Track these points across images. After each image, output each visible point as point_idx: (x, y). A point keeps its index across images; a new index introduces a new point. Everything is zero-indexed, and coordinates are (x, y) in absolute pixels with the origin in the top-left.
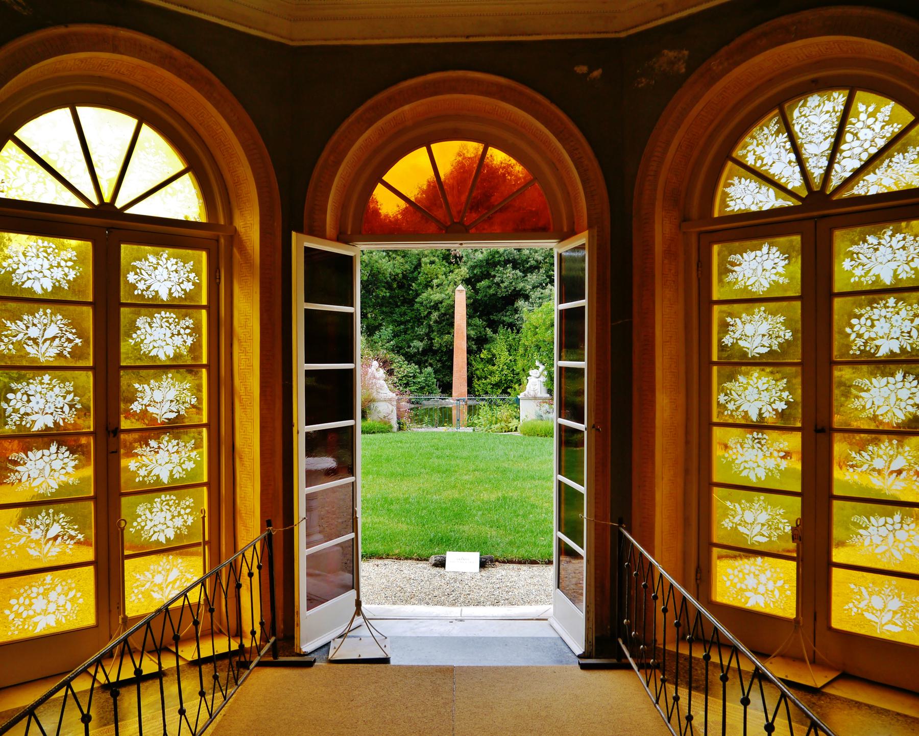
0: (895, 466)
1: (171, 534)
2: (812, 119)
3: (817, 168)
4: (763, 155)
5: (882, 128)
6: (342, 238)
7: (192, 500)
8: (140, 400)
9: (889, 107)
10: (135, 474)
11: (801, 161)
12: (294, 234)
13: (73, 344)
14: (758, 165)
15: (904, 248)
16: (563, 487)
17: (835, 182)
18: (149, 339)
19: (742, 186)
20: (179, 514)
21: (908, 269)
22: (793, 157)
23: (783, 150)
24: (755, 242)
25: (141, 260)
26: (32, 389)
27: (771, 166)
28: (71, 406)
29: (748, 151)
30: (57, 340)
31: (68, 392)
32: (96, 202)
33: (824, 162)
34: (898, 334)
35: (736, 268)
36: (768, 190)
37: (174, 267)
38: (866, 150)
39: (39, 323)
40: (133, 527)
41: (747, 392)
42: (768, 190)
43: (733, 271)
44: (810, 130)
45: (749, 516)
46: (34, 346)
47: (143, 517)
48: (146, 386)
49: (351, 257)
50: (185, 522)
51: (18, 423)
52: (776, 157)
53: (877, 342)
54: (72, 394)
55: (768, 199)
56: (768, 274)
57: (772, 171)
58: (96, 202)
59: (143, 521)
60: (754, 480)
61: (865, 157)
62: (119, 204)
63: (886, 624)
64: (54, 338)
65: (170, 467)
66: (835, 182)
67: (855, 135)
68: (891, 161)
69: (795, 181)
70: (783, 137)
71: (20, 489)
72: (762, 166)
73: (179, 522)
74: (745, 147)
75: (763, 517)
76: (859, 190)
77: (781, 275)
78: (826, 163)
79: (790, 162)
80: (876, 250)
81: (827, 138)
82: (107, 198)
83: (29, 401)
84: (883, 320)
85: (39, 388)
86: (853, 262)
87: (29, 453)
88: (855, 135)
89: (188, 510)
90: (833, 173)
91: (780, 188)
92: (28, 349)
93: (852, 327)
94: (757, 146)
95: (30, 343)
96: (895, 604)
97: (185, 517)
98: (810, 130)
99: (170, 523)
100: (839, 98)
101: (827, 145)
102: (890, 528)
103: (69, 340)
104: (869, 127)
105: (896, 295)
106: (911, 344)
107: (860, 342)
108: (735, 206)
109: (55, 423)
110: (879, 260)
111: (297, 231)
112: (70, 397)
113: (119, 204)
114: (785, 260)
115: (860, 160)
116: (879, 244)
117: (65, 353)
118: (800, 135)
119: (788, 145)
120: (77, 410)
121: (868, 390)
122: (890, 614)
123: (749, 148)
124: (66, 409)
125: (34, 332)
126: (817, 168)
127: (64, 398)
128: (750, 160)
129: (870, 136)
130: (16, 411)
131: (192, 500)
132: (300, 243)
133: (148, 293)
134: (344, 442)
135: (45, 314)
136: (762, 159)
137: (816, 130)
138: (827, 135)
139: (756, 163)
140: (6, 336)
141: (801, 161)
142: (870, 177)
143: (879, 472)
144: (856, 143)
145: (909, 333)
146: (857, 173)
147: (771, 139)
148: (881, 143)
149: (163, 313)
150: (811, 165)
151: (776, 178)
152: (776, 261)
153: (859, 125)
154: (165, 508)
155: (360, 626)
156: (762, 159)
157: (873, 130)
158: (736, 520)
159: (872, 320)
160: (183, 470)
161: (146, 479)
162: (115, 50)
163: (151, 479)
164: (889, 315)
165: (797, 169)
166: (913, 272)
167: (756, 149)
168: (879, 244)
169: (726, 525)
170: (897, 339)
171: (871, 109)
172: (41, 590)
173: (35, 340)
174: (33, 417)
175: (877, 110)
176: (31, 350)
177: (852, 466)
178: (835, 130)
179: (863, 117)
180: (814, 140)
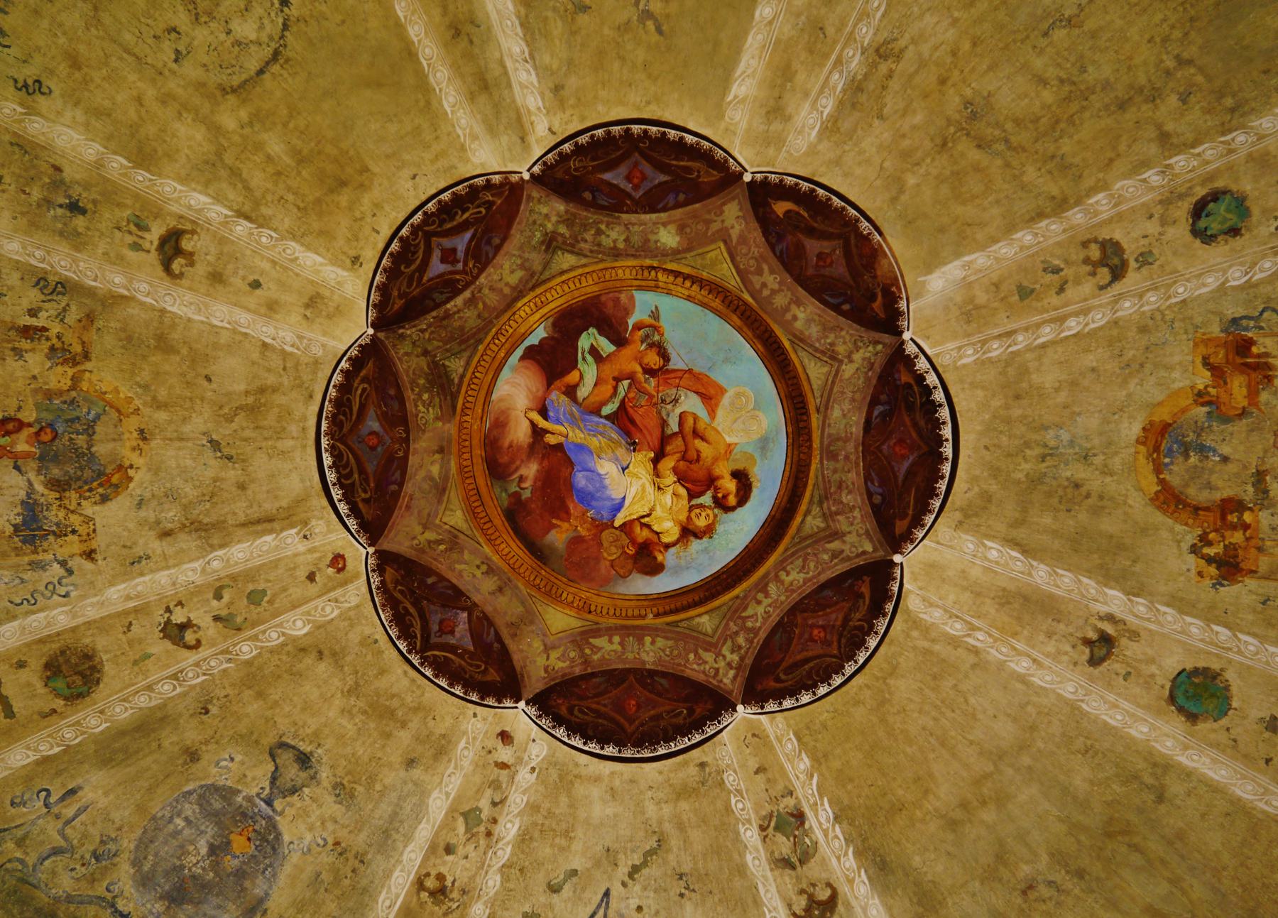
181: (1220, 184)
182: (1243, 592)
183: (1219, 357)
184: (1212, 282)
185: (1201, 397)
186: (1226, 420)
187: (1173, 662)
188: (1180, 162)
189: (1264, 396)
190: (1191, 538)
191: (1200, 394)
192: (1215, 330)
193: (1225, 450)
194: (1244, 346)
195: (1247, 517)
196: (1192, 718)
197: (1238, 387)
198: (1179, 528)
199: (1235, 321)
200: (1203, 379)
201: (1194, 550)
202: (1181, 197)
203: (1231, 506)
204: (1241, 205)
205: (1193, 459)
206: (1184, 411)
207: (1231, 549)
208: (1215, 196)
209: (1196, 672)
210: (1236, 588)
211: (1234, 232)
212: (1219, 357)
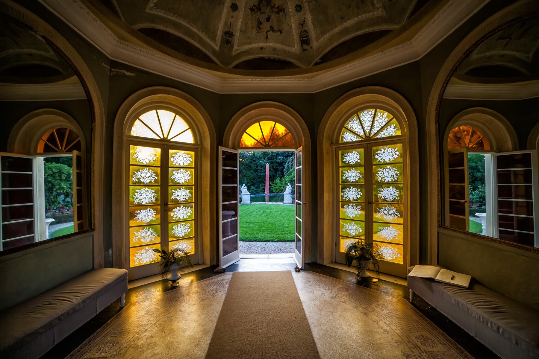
0: (390, 213)
1: (183, 234)
2: (366, 116)
3: (367, 130)
4: (353, 126)
5: (385, 119)
6: (234, 148)
7: (190, 224)
8: (174, 195)
9: (386, 114)
10: (173, 217)
11: (363, 128)
12: (219, 147)
13: (155, 179)
14: (351, 129)
15: (391, 152)
16: (297, 221)
17: (372, 134)
18: (177, 177)
20: (186, 229)
21: (393, 158)
22: (361, 127)
23: (358, 125)
24: (350, 151)
25: (175, 154)
26: (142, 192)
28: (154, 197)
29: (349, 125)
30: (150, 177)
31: (153, 193)
32: (162, 137)
33: (369, 128)
37: (185, 156)
38: (380, 125)
39: (145, 172)
40: (172, 232)
44: (365, 120)
45: (350, 227)
46: (143, 179)
47: (175, 229)
48: (176, 191)
49: (237, 154)
50: (188, 231)
51: (138, 202)
53: (385, 178)
54: (154, 193)
55: (354, 138)
56: (355, 159)
57: (355, 131)
58: (162, 137)
59: (175, 230)
60: (352, 217)
61: (380, 127)
62: (169, 138)
63: (388, 257)
64: (149, 177)
65: (183, 215)
66: (372, 134)
67: (377, 121)
68: (387, 128)
69: (362, 134)
70: (358, 121)
71: (138, 221)
72: (352, 129)
73: (186, 231)
74: (348, 123)
75: (354, 228)
76: (379, 136)
77: (358, 159)
78: (370, 129)
79: (360, 128)
80: (384, 153)
81: (370, 122)
82: (165, 136)
83: (141, 195)
84: (386, 172)
85: (144, 192)
86: (378, 156)
87: (141, 211)
88: (377, 121)
89: (189, 227)
91: (358, 135)
92: (141, 180)
93: (378, 174)
94: (351, 124)
95: (142, 178)
96: (390, 251)
97: (188, 229)
98: (365, 120)
99: (183, 231)
100: (373, 111)
101: (370, 124)
102: (389, 230)
103: (154, 178)
104: (381, 119)
105: (390, 165)
106: (394, 179)
107: (380, 178)
108: (345, 140)
109: (149, 202)
110: (385, 155)
111: (220, 146)
112: (153, 194)
113: (169, 138)
114: (359, 155)
115: (379, 128)
116: (385, 151)
117: (152, 181)
119: (359, 124)
120: (155, 198)
121: (383, 192)
122: (389, 254)
123: (349, 124)
124: (152, 198)
125: (143, 175)
126: (367, 130)
127: (152, 194)
128: (349, 127)
129: (381, 122)
130: (137, 198)
131: (190, 224)
132: (221, 149)
133: (177, 164)
134: (234, 208)
135: (147, 170)
136: (352, 127)
137: (367, 119)
140: (135, 176)
141: (363, 128)
142: (382, 133)
143: (386, 214)
144: (378, 123)
145: (393, 176)
146: (378, 132)
147: (355, 122)
148: (384, 123)
149: (181, 170)
150: (366, 129)
153: (378, 118)
154: (182, 227)
155: (239, 261)
156: (353, 127)
158: (347, 229)
159: (383, 172)
160: (187, 216)
161: (176, 218)
162: (169, 94)
163: (177, 218)
164: (388, 171)
165: (362, 130)
166: (394, 159)
168: (385, 151)
170: (390, 177)
171: (381, 114)
172: (145, 251)
173: (143, 177)
174: (143, 200)
175: (383, 114)
176: (142, 180)
177: (379, 213)
178: (372, 120)
179: (379, 116)
181: (303, 9)
182: (249, 11)
183: (280, 8)
184: (290, 7)
185: (275, 5)
186: (272, 8)
187: (238, 4)
188: (307, 4)
189: (275, 13)
190: (255, 5)
191: (275, 5)
192: (284, 7)
193: (267, 8)
194: (281, 11)
195: (259, 12)
196: (231, 7)
197: (276, 10)
198: (257, 3)
199: (284, 10)
200: (277, 5)
201: (254, 5)
202: (302, 4)
203: (260, 10)
204: (299, 11)
205: (266, 4)
206: (273, 3)
207: (254, 10)
208: (301, 8)
209: (237, 7)
210: (249, 10)
211: (296, 10)
212: (280, 8)
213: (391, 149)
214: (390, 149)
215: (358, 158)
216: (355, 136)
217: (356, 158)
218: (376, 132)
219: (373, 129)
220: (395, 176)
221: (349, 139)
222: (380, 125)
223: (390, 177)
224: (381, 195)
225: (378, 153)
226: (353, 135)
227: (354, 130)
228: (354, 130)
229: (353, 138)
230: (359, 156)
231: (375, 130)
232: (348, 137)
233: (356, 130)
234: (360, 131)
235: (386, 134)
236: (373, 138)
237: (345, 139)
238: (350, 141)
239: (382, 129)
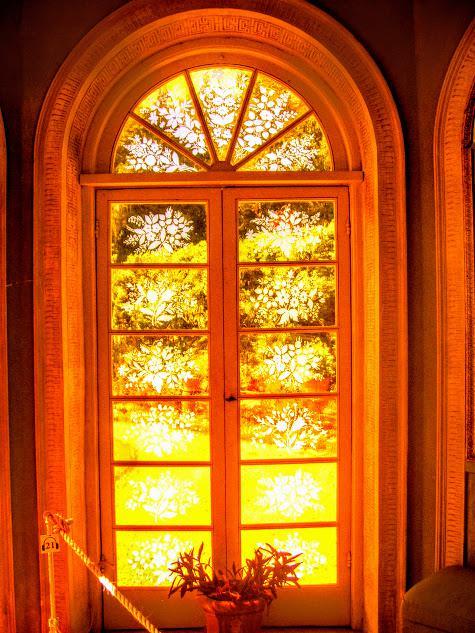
4: (167, 118)
5: (281, 113)
9: (288, 96)
11: (206, 130)
15: (300, 225)
19: (144, 146)
22: (198, 125)
23: (187, 116)
27: (175, 130)
33: (229, 135)
34: (297, 304)
35: (137, 231)
36: (172, 153)
38: (267, 130)
41: (150, 363)
42: (172, 153)
43: (133, 234)
52: (181, 122)
57: (176, 135)
61: (266, 136)
78: (230, 136)
79: (195, 129)
90: (237, 146)
104: (269, 109)
115: (262, 138)
116: (280, 219)
118: (205, 104)
119: (193, 112)
129: (270, 117)
136: (166, 121)
137: (222, 101)
138: (231, 109)
139: (159, 124)
141: (206, 130)
144: (258, 122)
145: (306, 303)
148: (281, 126)
150: (216, 133)
151: (181, 142)
152: (181, 226)
153: (261, 106)
157: (273, 113)
158: (142, 498)
165: (202, 137)
167: (160, 110)
169: (130, 506)
170: (297, 308)
175: (277, 95)
180: (219, 110)
213: (301, 216)
214: (297, 214)
215: (185, 235)
216: (175, 157)
217: (178, 237)
218: (251, 150)
219: (240, 140)
220: (310, 304)
221: (151, 161)
222: (267, 130)
223: (297, 308)
224: (267, 370)
225: (255, 225)
226: (168, 152)
227: (171, 131)
228: (171, 131)
229: (167, 162)
230: (187, 230)
231: (251, 141)
232: (143, 156)
233: (180, 134)
234: (192, 138)
235: (286, 162)
236: (242, 169)
237: (133, 162)
238: (156, 169)
239: (271, 143)
